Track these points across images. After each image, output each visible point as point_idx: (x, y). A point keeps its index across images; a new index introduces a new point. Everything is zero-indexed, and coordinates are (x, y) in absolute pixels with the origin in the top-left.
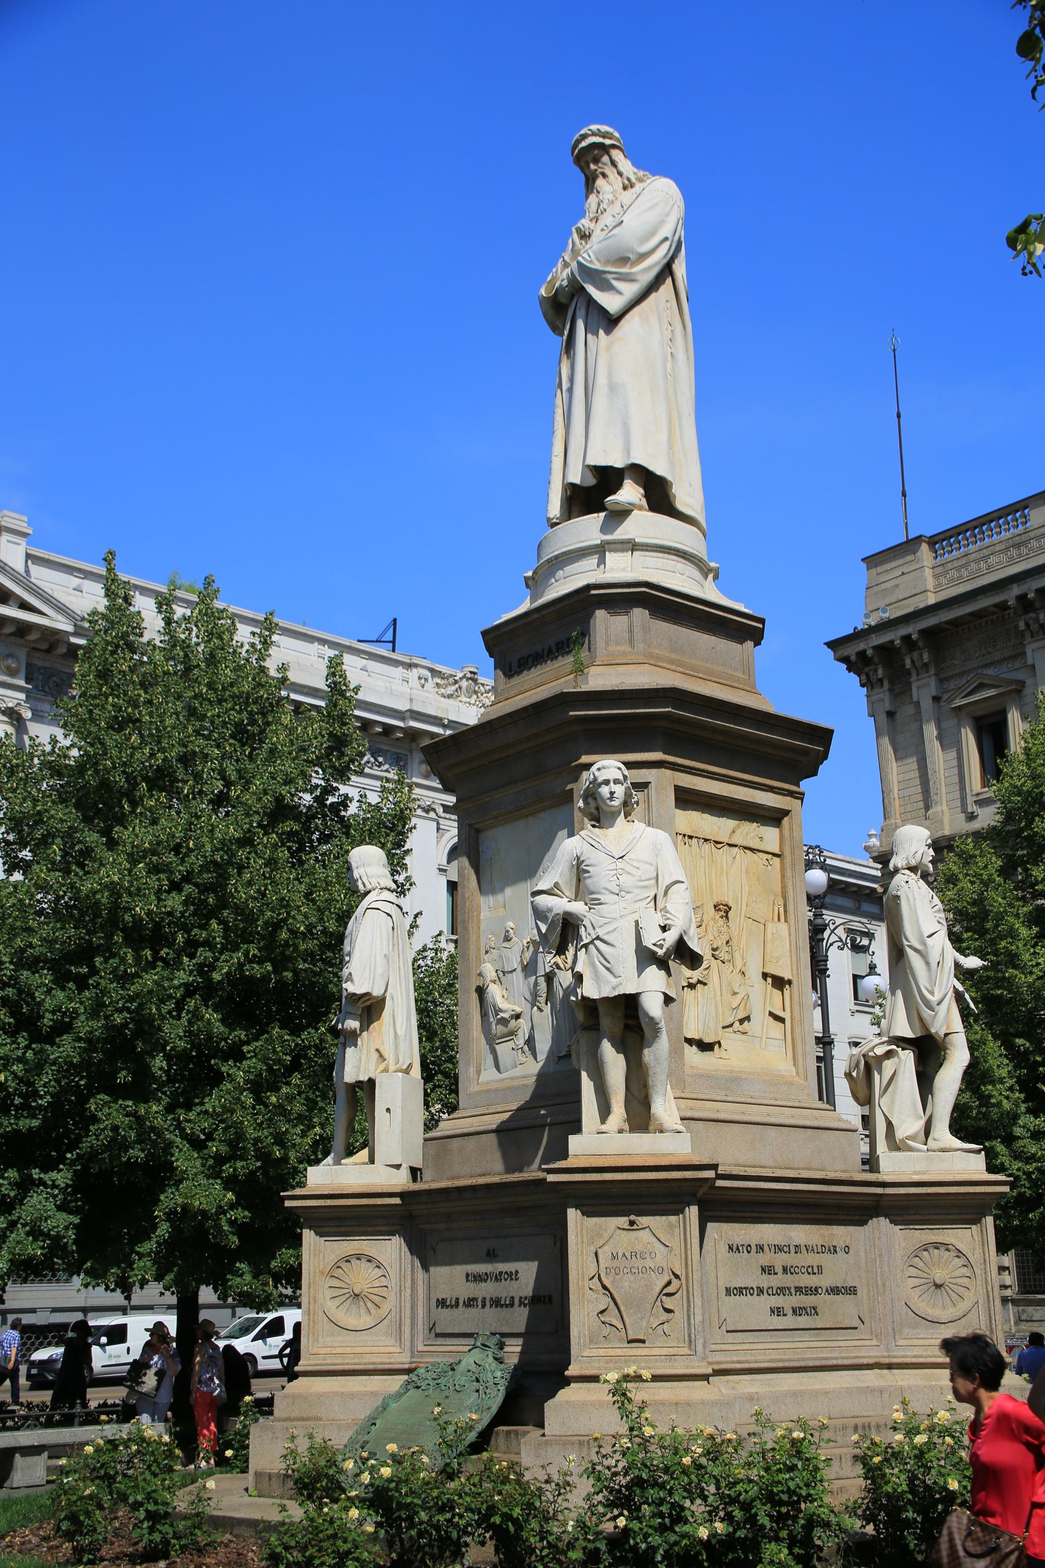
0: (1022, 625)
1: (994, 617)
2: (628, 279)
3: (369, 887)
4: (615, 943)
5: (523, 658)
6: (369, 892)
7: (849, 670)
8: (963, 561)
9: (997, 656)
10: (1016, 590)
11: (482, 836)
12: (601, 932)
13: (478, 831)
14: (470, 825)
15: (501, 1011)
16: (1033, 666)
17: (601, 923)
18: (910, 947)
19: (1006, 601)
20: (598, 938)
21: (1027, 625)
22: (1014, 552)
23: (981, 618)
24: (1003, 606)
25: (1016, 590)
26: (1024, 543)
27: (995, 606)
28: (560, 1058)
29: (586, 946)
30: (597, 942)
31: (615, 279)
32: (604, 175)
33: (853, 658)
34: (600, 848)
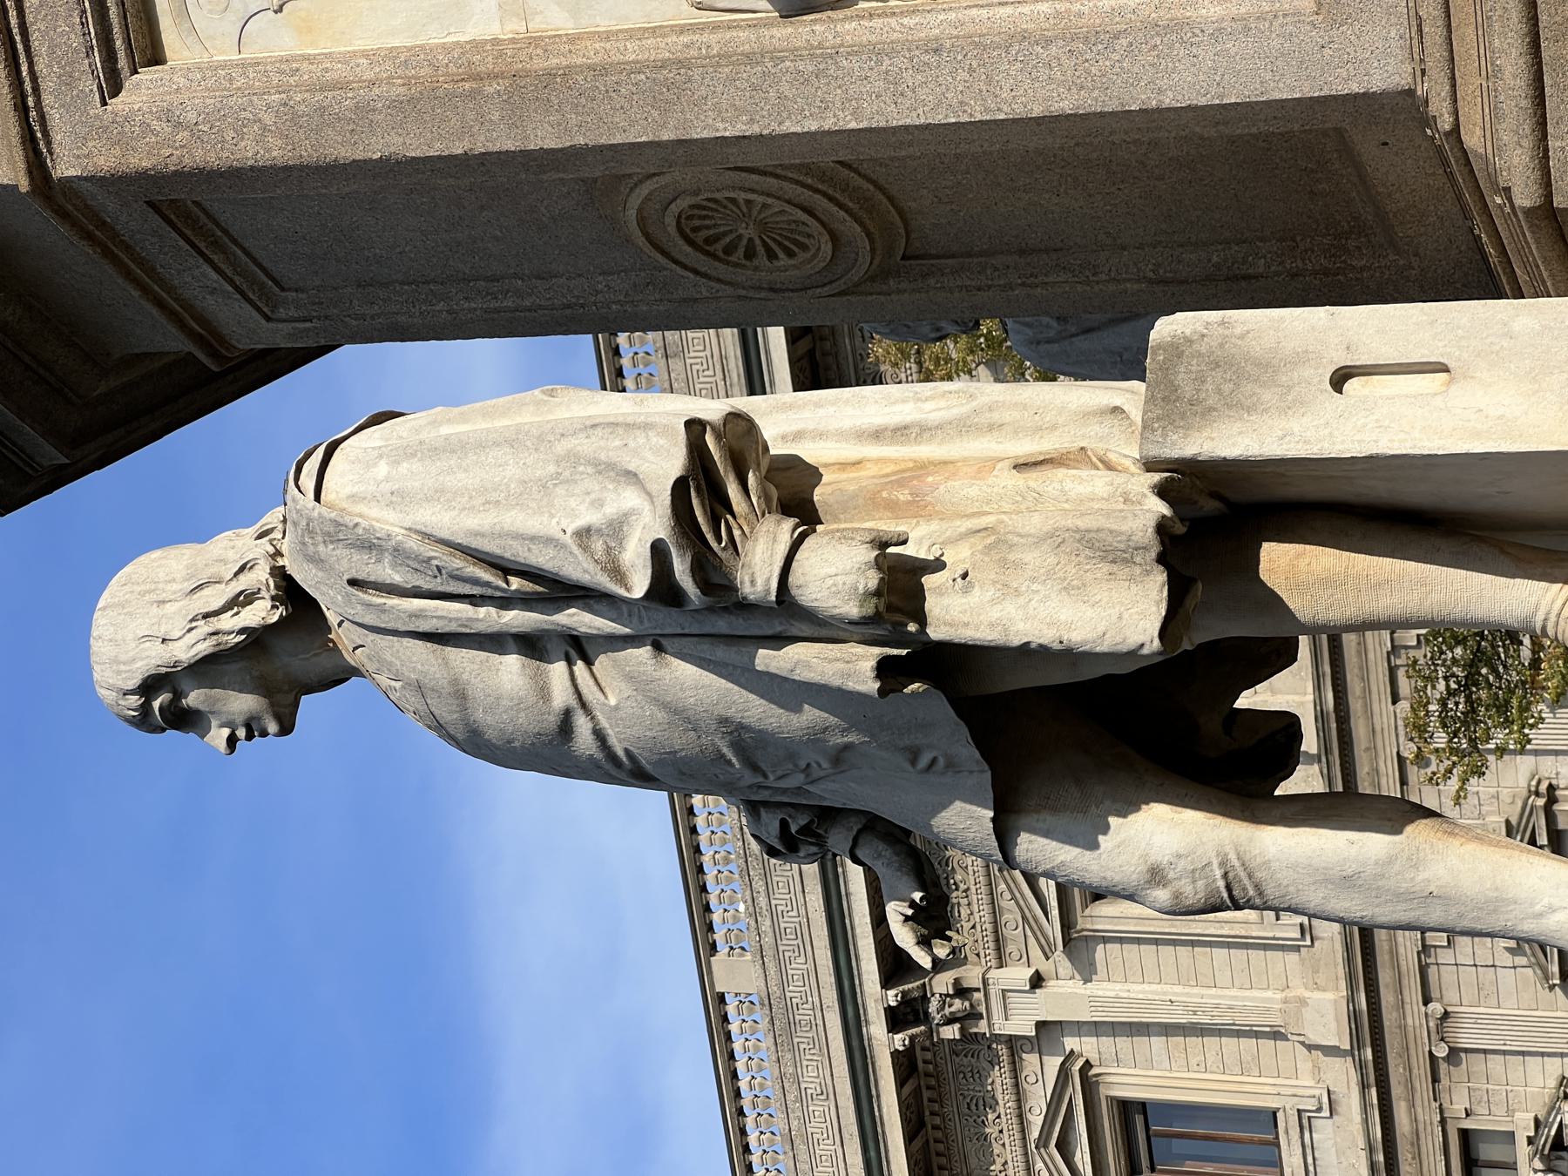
0: (951, 1032)
1: (926, 1094)
3: (261, 575)
6: (280, 574)
8: (801, 1148)
9: (1005, 1102)
10: (877, 1029)
16: (1041, 1025)
19: (895, 1055)
21: (950, 1021)
22: (802, 1038)
23: (922, 1124)
24: (905, 1064)
25: (877, 1029)
26: (788, 1008)
27: (900, 1083)
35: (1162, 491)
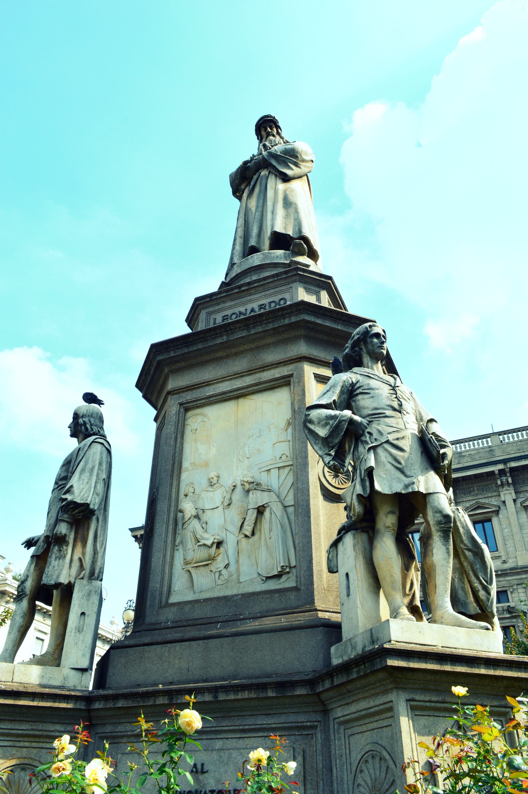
2: (296, 164)
4: (405, 448)
5: (227, 315)
7: (136, 541)
11: (190, 413)
12: (391, 438)
13: (187, 410)
14: (181, 404)
15: (203, 538)
17: (390, 431)
18: (467, 549)
20: (388, 442)
28: (268, 578)
29: (374, 448)
30: (387, 446)
31: (290, 163)
32: (274, 136)
33: (139, 536)
34: (377, 378)
35: (70, 582)
